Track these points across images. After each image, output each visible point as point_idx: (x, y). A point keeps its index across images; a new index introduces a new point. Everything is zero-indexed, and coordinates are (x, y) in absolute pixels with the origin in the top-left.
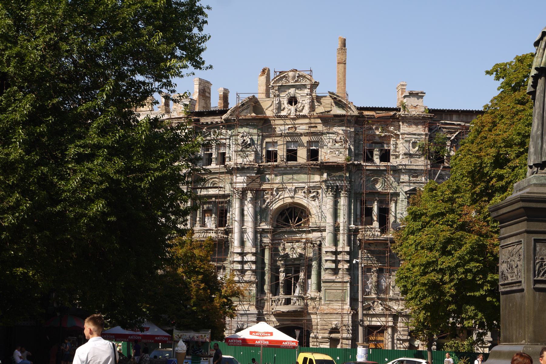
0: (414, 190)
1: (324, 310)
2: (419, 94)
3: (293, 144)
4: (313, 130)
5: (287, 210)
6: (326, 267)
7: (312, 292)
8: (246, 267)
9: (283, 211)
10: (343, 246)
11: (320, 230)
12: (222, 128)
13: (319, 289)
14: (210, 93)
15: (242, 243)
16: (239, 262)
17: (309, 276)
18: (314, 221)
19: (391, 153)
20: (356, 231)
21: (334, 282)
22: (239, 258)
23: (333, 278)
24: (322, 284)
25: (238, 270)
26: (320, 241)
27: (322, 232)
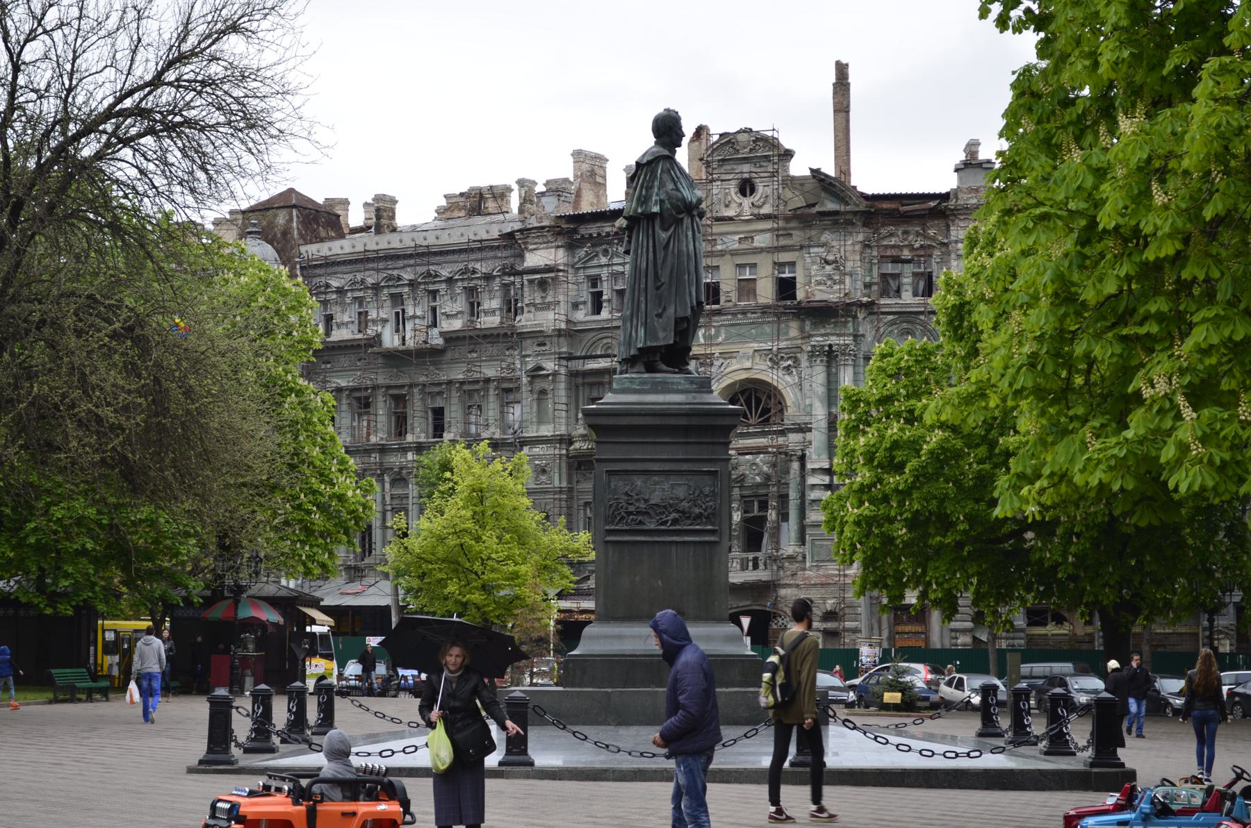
2: (984, 166)
3: (748, 269)
4: (783, 242)
5: (742, 392)
7: (789, 547)
9: (736, 394)
11: (803, 429)
13: (802, 540)
14: (604, 177)
17: (784, 517)
18: (792, 413)
24: (808, 531)
26: (802, 450)
27: (805, 432)
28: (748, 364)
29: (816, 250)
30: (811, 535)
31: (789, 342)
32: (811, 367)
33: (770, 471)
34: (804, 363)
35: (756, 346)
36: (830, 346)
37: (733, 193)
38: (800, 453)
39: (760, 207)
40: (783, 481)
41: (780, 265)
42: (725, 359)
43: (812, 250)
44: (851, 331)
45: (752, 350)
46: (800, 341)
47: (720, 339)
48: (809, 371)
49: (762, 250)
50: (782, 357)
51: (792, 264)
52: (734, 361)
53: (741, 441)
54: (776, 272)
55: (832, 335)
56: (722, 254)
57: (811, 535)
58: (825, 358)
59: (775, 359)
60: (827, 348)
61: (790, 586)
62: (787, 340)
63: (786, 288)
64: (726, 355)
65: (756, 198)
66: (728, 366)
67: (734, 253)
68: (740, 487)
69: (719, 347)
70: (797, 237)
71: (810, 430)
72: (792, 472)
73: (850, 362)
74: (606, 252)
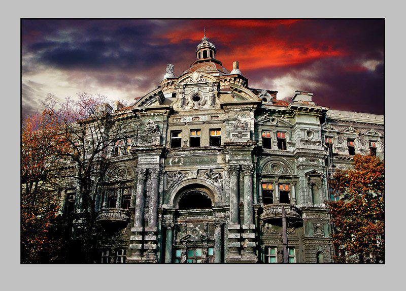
0: (314, 172)
8: (146, 246)
11: (224, 209)
15: (144, 223)
16: (140, 242)
19: (288, 140)
20: (260, 211)
22: (140, 238)
29: (232, 122)
32: (229, 177)
33: (204, 234)
36: (240, 166)
38: (222, 223)
43: (230, 122)
46: (223, 165)
47: (180, 164)
50: (213, 173)
55: (242, 160)
60: (238, 167)
63: (215, 141)
65: (201, 102)
66: (184, 177)
67: (190, 124)
68: (187, 242)
70: (222, 117)
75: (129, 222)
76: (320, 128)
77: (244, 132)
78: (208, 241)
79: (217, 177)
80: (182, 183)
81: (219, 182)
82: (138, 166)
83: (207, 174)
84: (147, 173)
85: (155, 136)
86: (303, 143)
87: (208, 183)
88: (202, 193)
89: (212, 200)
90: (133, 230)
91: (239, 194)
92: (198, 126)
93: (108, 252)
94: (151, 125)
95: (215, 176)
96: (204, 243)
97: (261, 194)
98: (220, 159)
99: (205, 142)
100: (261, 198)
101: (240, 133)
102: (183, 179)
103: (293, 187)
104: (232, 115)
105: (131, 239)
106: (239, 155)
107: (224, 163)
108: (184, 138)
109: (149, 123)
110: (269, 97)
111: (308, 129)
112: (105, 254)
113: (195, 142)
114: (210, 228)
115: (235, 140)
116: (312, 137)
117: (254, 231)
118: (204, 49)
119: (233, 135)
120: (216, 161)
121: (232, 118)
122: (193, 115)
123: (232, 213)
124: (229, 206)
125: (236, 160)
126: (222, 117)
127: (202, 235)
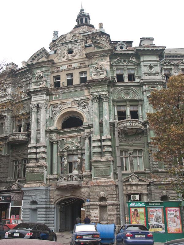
1: (93, 183)
2: (150, 39)
6: (94, 151)
10: (107, 135)
11: (90, 127)
12: (28, 74)
13: (90, 169)
15: (38, 140)
18: (86, 122)
19: (135, 75)
21: (100, 161)
22: (34, 150)
23: (100, 159)
25: (34, 159)
28: (70, 106)
29: (94, 65)
30: (93, 166)
31: (85, 97)
33: (79, 145)
34: (90, 103)
35: (73, 99)
36: (100, 95)
37: (65, 53)
38: (89, 136)
39: (75, 56)
40: (83, 148)
41: (81, 73)
42: (62, 105)
43: (92, 66)
44: (107, 90)
45: (71, 101)
47: (60, 98)
48: (92, 106)
49: (75, 68)
50: (82, 103)
51: (85, 72)
52: (65, 106)
53: (67, 135)
54: (80, 76)
55: (100, 91)
56: (62, 71)
57: (93, 166)
58: (98, 100)
59: (79, 104)
60: (98, 96)
61: (85, 187)
62: (84, 96)
63: (83, 80)
64: (63, 104)
65: (73, 54)
67: (65, 70)
69: (60, 101)
71: (92, 127)
72: (86, 143)
73: (107, 101)
74: (25, 78)
75: (28, 141)
76: (159, 63)
77: (101, 71)
78: (81, 149)
79: (85, 105)
80: (62, 111)
81: (87, 108)
82: (32, 103)
83: (78, 104)
84: (38, 107)
85: (42, 81)
86: (146, 75)
87: (79, 110)
88: (77, 117)
89: (83, 121)
90: (30, 146)
91: (101, 115)
92: (71, 71)
93: (17, 163)
94: (39, 74)
95: (83, 105)
96: (79, 151)
97: (116, 114)
98: (86, 93)
99: (76, 81)
100: (116, 117)
101: (99, 72)
102: (62, 109)
103: (140, 107)
104: (94, 61)
105: (28, 152)
106: (99, 88)
107: (89, 94)
108: (63, 81)
109: (38, 73)
110: (125, 45)
111: (150, 64)
112: (16, 164)
113: (70, 82)
114: (83, 138)
115: (95, 77)
116: (153, 70)
117: (110, 140)
118: (81, 18)
119: (94, 74)
120: (84, 94)
121: (93, 63)
122: (68, 64)
123: (96, 128)
124: (93, 124)
125: (97, 92)
126: (87, 63)
127: (77, 146)
